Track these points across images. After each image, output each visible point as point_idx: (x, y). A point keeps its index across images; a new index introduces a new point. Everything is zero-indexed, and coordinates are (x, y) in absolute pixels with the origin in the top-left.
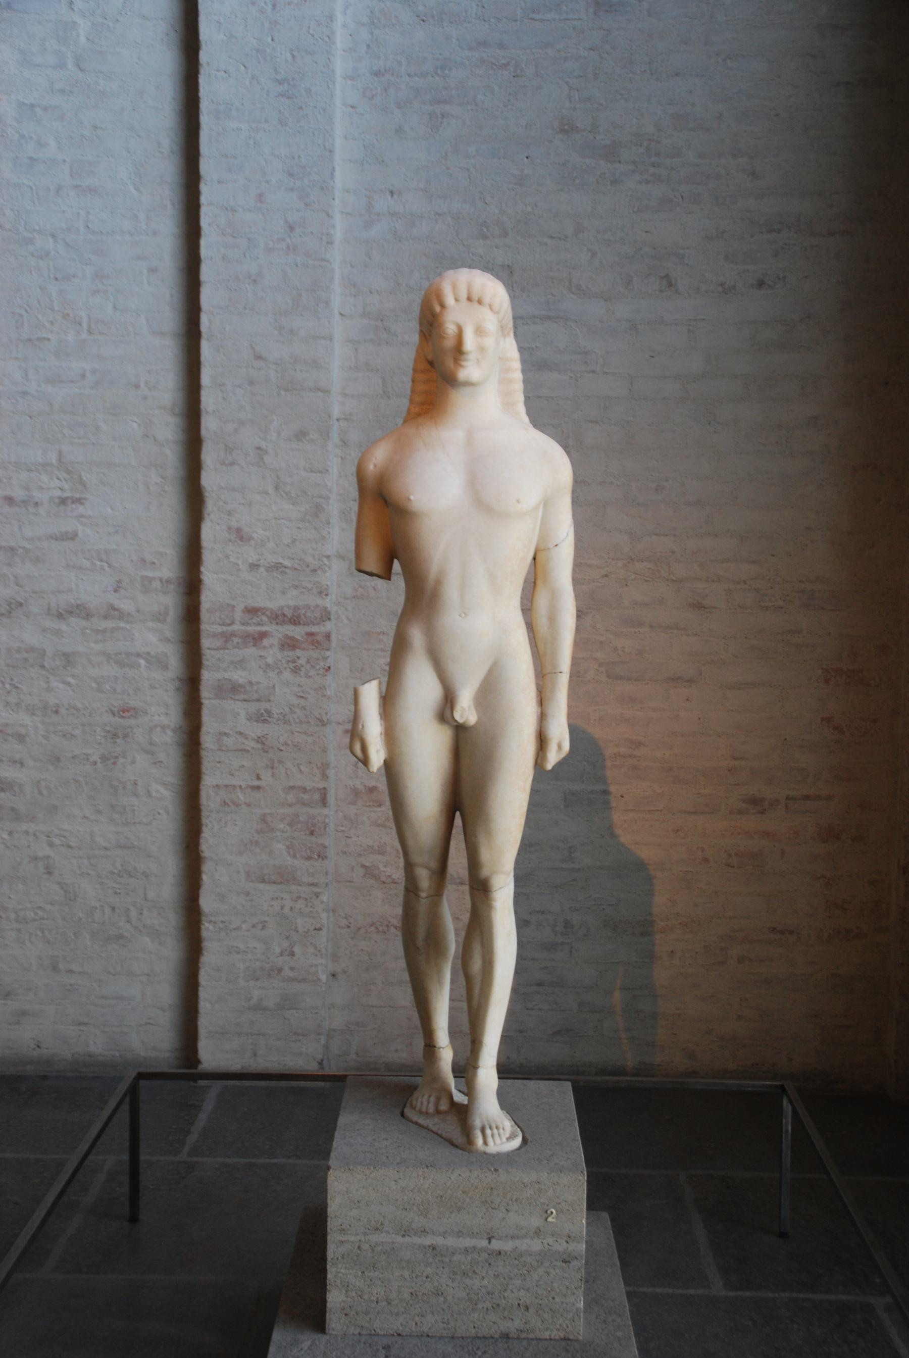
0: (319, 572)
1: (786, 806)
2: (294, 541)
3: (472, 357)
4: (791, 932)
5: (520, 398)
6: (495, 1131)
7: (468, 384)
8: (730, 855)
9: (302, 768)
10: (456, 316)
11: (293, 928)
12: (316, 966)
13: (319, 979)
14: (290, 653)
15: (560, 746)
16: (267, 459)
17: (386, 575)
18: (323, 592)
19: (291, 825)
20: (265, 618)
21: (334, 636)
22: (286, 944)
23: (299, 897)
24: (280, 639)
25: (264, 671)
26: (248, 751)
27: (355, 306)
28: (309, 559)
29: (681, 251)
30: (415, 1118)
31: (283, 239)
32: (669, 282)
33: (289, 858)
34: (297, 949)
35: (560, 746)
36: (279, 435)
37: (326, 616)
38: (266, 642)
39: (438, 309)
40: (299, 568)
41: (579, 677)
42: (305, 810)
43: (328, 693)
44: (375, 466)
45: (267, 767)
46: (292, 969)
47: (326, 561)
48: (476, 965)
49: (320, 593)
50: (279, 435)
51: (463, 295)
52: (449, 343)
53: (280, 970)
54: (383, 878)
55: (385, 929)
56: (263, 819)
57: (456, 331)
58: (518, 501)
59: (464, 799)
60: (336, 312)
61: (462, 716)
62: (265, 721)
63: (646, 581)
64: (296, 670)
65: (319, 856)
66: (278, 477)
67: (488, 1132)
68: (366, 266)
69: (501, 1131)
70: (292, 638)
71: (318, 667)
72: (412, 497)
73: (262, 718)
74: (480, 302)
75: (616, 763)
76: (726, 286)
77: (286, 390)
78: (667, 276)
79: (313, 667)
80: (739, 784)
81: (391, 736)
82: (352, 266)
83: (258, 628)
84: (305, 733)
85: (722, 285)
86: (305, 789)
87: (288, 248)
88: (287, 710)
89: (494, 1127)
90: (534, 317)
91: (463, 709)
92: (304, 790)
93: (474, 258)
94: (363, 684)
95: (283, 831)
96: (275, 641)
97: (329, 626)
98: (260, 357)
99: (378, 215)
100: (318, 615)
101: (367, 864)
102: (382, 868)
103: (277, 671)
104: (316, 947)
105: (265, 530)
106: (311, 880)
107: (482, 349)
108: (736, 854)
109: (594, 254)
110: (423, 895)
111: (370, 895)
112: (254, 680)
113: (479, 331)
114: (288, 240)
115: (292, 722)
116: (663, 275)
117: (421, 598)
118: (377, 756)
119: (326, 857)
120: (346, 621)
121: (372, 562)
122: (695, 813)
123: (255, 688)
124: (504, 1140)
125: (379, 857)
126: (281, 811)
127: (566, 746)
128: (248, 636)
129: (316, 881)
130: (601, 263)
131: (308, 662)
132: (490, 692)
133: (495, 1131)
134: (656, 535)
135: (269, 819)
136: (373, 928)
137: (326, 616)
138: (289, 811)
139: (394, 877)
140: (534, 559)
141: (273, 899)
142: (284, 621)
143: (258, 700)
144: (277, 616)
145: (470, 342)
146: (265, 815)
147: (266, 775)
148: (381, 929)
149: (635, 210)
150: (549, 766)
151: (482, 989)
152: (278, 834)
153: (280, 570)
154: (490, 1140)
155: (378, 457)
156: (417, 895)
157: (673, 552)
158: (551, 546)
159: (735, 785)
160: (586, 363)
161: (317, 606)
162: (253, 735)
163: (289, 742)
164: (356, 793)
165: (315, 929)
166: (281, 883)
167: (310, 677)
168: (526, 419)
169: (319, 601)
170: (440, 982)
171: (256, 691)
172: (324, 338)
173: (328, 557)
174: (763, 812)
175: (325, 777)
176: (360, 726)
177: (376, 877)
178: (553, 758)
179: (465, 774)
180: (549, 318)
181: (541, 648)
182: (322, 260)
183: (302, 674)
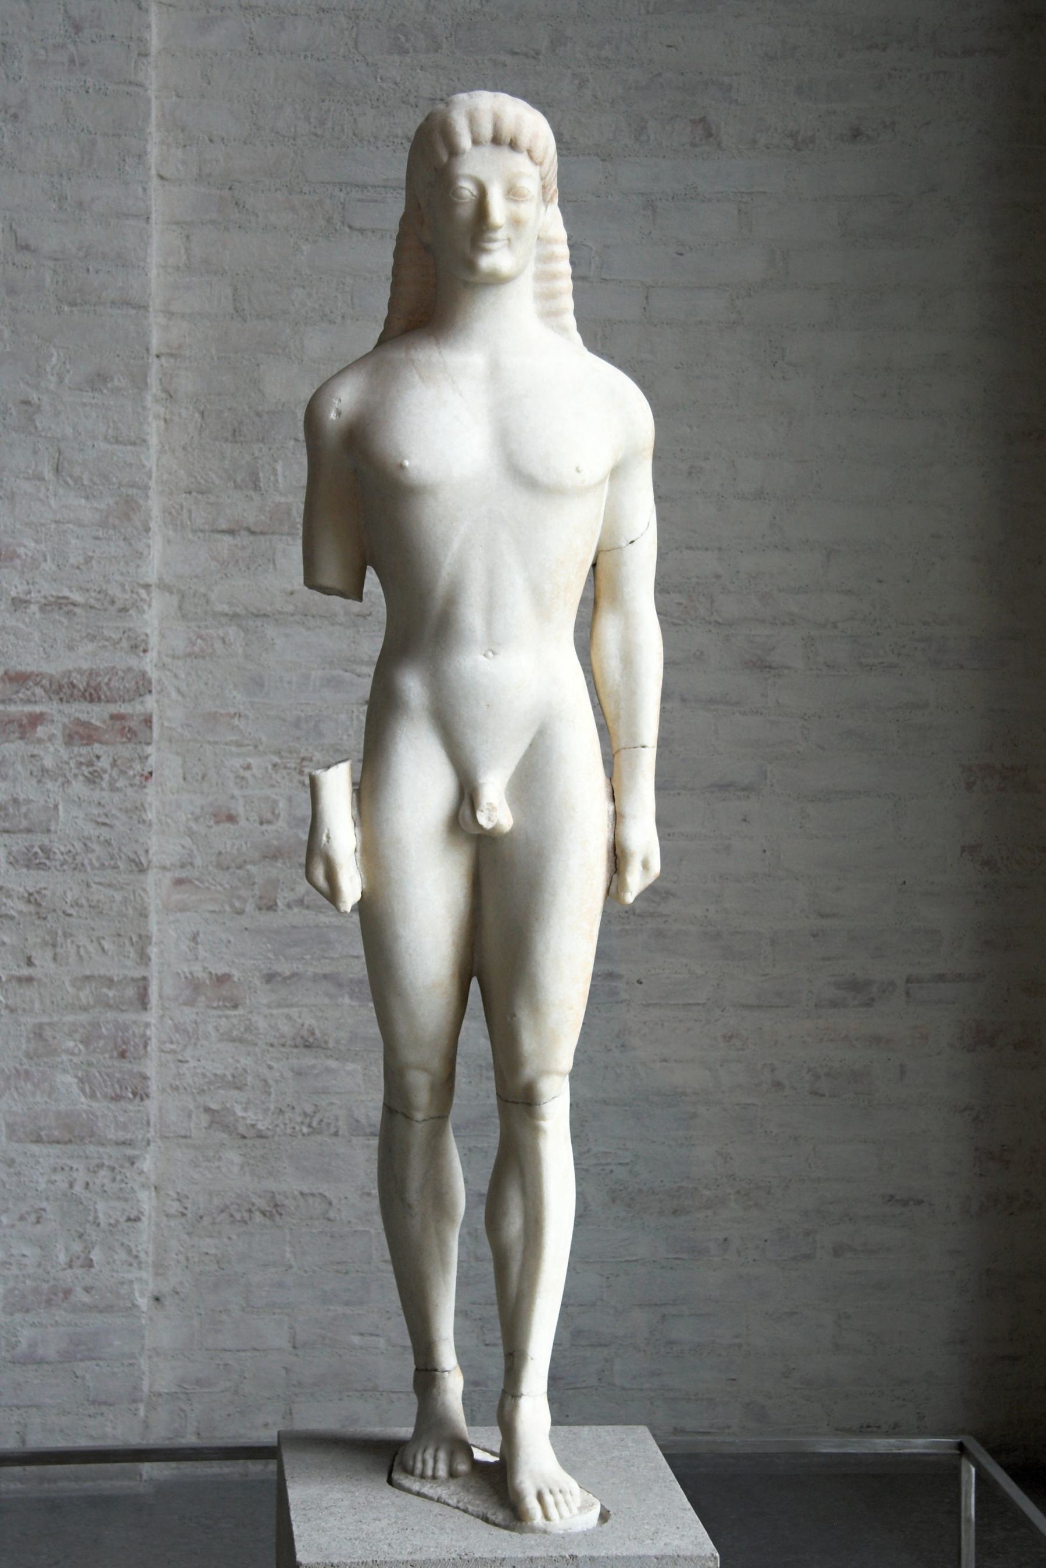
0: (132, 612)
1: (908, 993)
2: (88, 560)
3: (501, 235)
4: (920, 1202)
5: (568, 303)
6: (560, 1497)
7: (496, 280)
8: (817, 1077)
9: (106, 945)
10: (476, 166)
11: (91, 1218)
12: (131, 1282)
13: (135, 1306)
14: (84, 750)
15: (645, 865)
16: (40, 421)
18: (138, 646)
19: (86, 1042)
20: (38, 691)
21: (155, 719)
22: (77, 1247)
23: (101, 1166)
24: (65, 726)
25: (39, 782)
26: (12, 918)
27: (184, 163)
28: (113, 590)
29: (726, 80)
30: (416, 1486)
31: (63, 46)
32: (706, 130)
33: (83, 1099)
34: (96, 1255)
35: (645, 865)
36: (61, 380)
37: (143, 686)
38: (41, 731)
39: (445, 158)
40: (98, 606)
42: (110, 1015)
43: (150, 816)
44: (339, 413)
45: (45, 943)
46: (87, 1290)
47: (143, 593)
48: (514, 1225)
49: (134, 647)
50: (61, 380)
51: (486, 131)
52: (466, 211)
53: (68, 1293)
54: (242, 1130)
55: (246, 1215)
56: (38, 1033)
57: (475, 193)
58: (578, 471)
59: (495, 953)
60: (153, 172)
61: (489, 819)
62: (41, 866)
63: (674, 624)
64: (93, 779)
65: (135, 1094)
66: (60, 452)
67: (549, 1499)
68: (203, 96)
69: (569, 1496)
70: (87, 725)
71: (131, 773)
72: (407, 463)
73: (34, 860)
74: (513, 145)
75: (627, 927)
76: (800, 138)
77: (73, 304)
78: (703, 120)
79: (123, 772)
80: (829, 959)
82: (178, 96)
83: (28, 708)
84: (110, 885)
85: (793, 135)
86: (110, 981)
87: (72, 61)
88: (79, 846)
89: (556, 1490)
91: (492, 808)
92: (110, 982)
93: (385, 85)
94: (328, 767)
95: (73, 1054)
96: (56, 730)
97: (150, 703)
98: (27, 248)
99: (222, 9)
100: (131, 685)
101: (214, 1106)
102: (240, 1113)
103: (60, 780)
104: (129, 1251)
105: (37, 542)
106: (121, 1135)
107: (516, 223)
108: (827, 1075)
110: (419, 1116)
111: (220, 1159)
112: (22, 797)
113: (513, 193)
114: (72, 48)
115: (89, 868)
116: (697, 118)
117: (418, 627)
118: (351, 888)
119: (147, 1096)
120: (174, 695)
122: (760, 1007)
123: (24, 809)
124: (575, 1511)
125: (234, 1093)
126: (69, 1018)
127: (656, 867)
128: (11, 722)
129: (129, 1136)
130: (595, 97)
131: (114, 764)
132: (531, 780)
133: (560, 1497)
134: (691, 548)
135: (48, 1033)
136: (224, 1216)
137: (143, 686)
138: (83, 1018)
139: (260, 1126)
140: (594, 565)
141: (55, 1170)
142: (72, 695)
143: (29, 831)
144: (61, 687)
145: (498, 209)
146: (41, 1026)
147: (43, 959)
148: (238, 1216)
149: (650, 9)
150: (630, 898)
151: (523, 1265)
152: (65, 1057)
153: (65, 609)
154: (553, 1512)
155: (345, 399)
156: (408, 1117)
157: (718, 577)
158: (624, 544)
159: (824, 959)
161: (130, 669)
162: (21, 890)
163: (84, 901)
164: (195, 986)
165: (129, 1219)
166: (70, 1141)
167: (118, 790)
168: (578, 338)
169: (133, 662)
170: (444, 1264)
171: (26, 816)
172: (136, 216)
173: (147, 587)
174: (869, 1003)
175: (144, 958)
176: (324, 838)
177: (226, 1128)
178: (636, 883)
179: (490, 914)
181: (609, 708)
182: (131, 83)
183: (105, 784)
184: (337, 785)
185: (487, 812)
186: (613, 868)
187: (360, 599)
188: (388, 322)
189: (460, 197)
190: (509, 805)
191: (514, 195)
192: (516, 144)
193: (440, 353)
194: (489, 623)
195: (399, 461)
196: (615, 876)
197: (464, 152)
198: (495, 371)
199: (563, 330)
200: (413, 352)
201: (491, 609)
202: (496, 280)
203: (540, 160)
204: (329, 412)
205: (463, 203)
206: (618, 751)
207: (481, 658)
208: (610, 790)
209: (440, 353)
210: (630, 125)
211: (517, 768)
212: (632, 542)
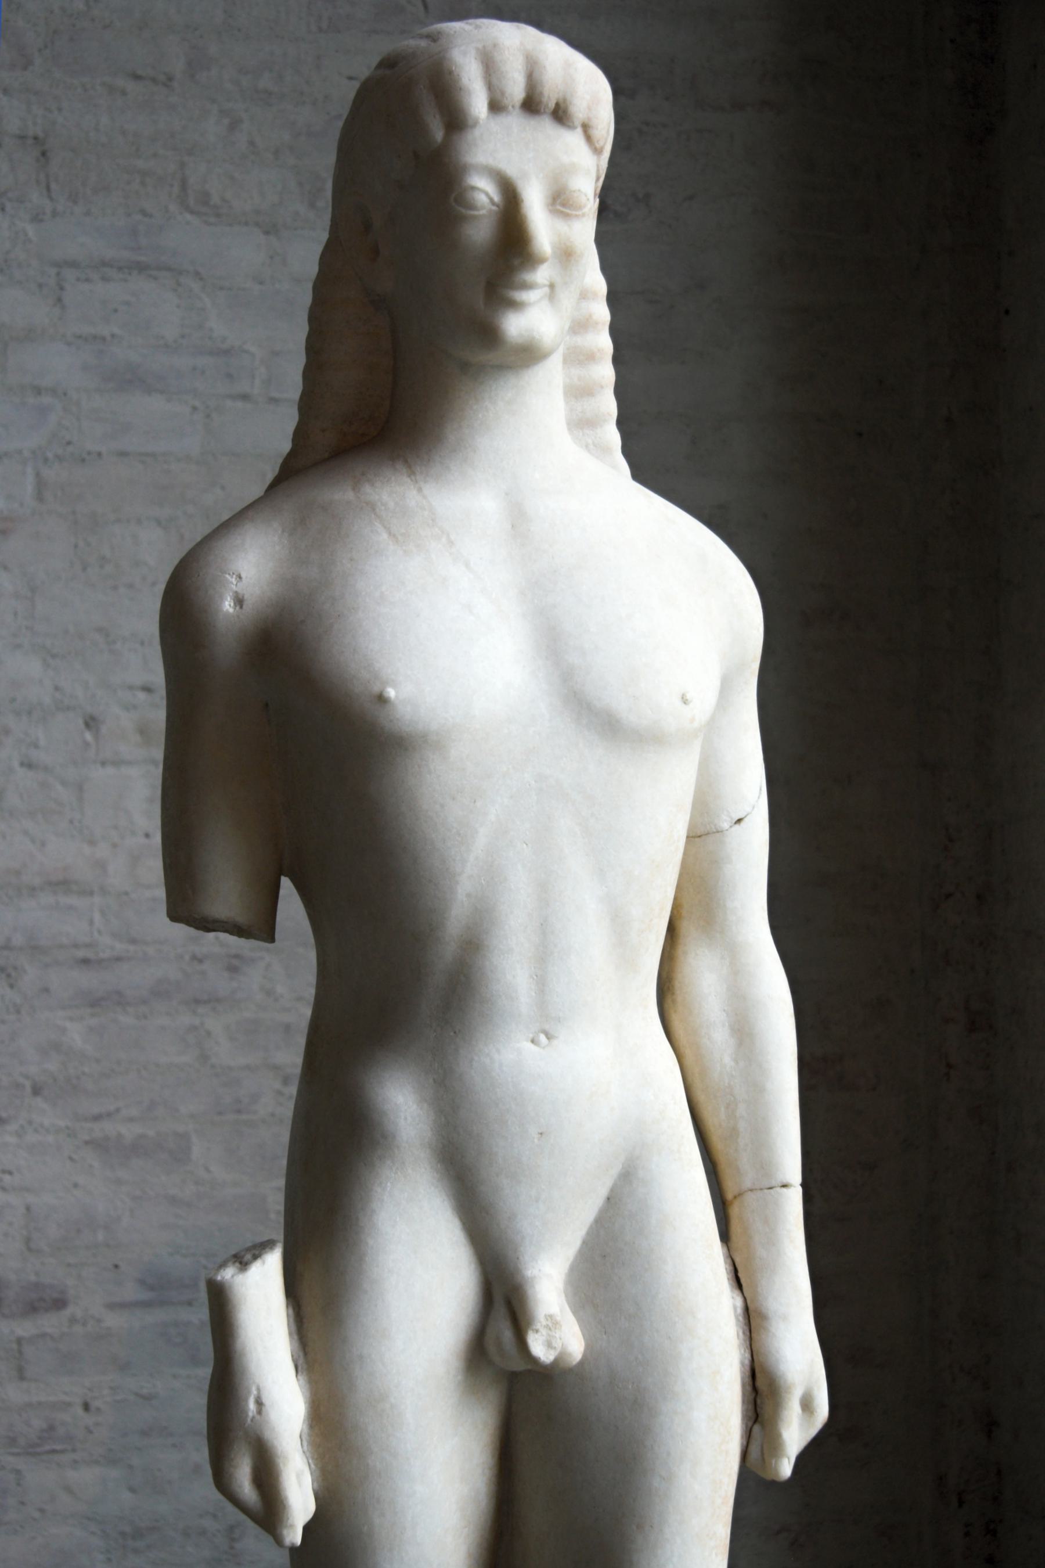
3: (542, 275)
7: (529, 354)
15: (807, 1405)
17: (263, 928)
35: (807, 1405)
41: (239, 1112)
44: (239, 601)
51: (516, 90)
52: (480, 232)
57: (497, 198)
58: (685, 701)
61: (549, 1345)
72: (391, 693)
74: (560, 115)
81: (334, 1425)
90: (104, 264)
91: (554, 1323)
107: (567, 255)
109: (234, 125)
113: (560, 202)
118: (300, 1501)
121: (226, 892)
130: (252, 143)
150: (786, 1469)
155: (248, 574)
158: (725, 825)
160: (229, 376)
180: (141, 268)
184: (261, 1293)
185: (544, 1331)
186: (751, 1413)
187: (270, 937)
188: (300, 435)
189: (472, 207)
190: (575, 1313)
191: (564, 205)
192: (565, 112)
193: (420, 490)
194: (542, 984)
195: (376, 689)
196: (757, 1428)
197: (476, 123)
198: (518, 521)
199: (600, 450)
200: (367, 489)
201: (544, 956)
202: (529, 354)
203: (601, 143)
204: (222, 598)
205: (475, 217)
206: (739, 1195)
207: (528, 1046)
208: (732, 1268)
209: (420, 490)
211: (585, 1243)
212: (739, 821)
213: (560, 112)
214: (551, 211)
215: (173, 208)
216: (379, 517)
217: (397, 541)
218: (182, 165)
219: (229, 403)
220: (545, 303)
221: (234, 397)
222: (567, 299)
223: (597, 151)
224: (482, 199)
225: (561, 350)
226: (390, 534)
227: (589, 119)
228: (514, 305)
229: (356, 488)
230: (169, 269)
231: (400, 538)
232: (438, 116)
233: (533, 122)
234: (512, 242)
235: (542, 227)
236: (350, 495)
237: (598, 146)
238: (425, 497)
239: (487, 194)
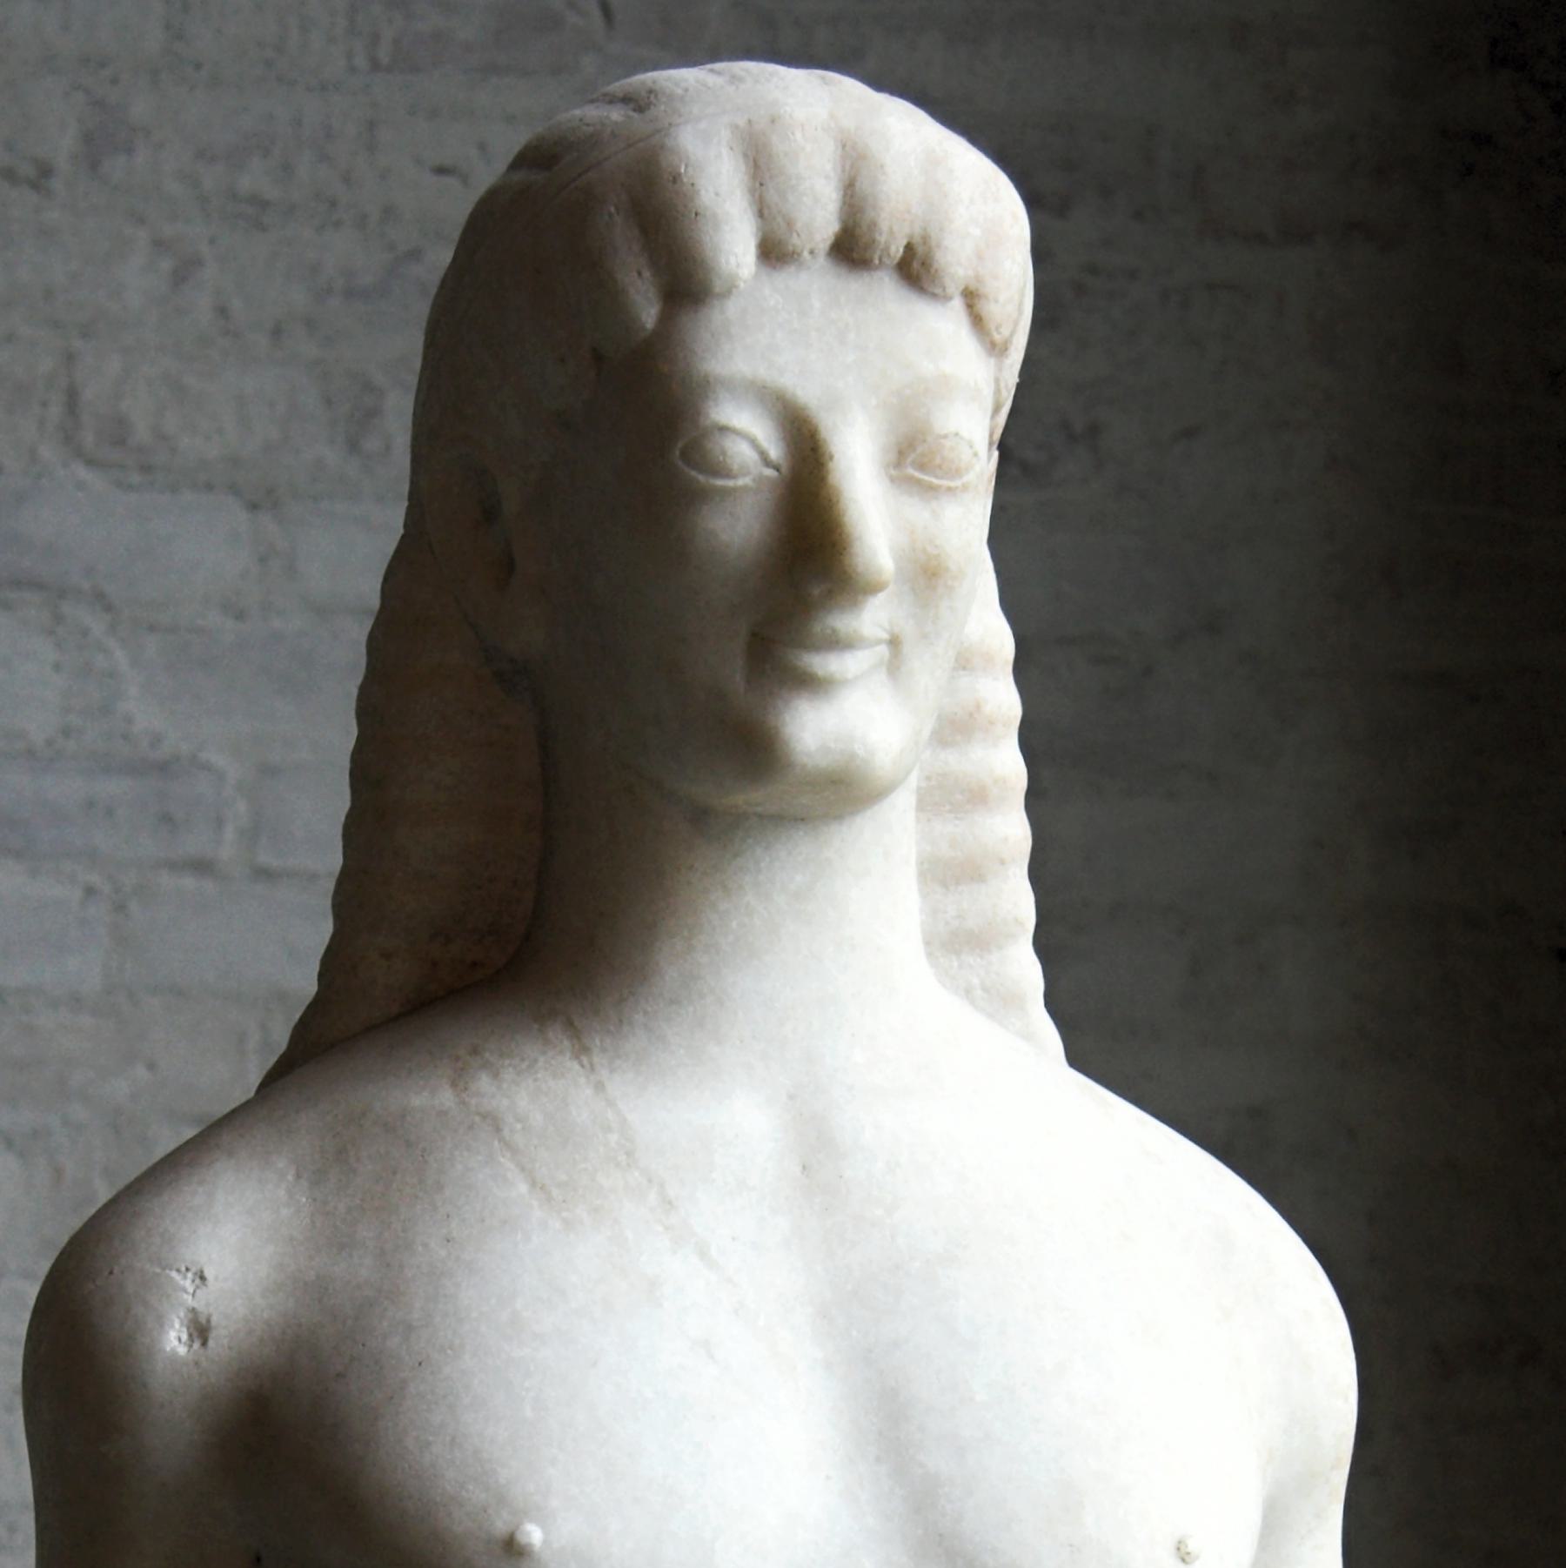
3: (871, 619)
7: (843, 792)
39: (648, 313)
51: (819, 218)
52: (737, 524)
57: (775, 452)
74: (915, 270)
107: (928, 575)
113: (914, 459)
130: (222, 311)
160: (167, 819)
188: (335, 964)
191: (922, 467)
192: (926, 264)
193: (599, 1087)
200: (484, 1082)
202: (843, 792)
203: (1005, 332)
205: (726, 493)
209: (599, 1087)
210: (329, 402)
213: (916, 265)
214: (892, 480)
215: (47, 452)
216: (508, 1146)
217: (549, 1199)
218: (70, 358)
219: (166, 880)
220: (882, 676)
221: (174, 866)
222: (927, 670)
223: (996, 349)
224: (740, 454)
225: (913, 780)
226: (533, 1184)
227: (978, 279)
228: (809, 683)
229: (459, 1080)
230: (38, 585)
231: (555, 1192)
232: (647, 274)
233: (855, 285)
234: (808, 547)
235: (874, 514)
236: (446, 1097)
237: (997, 337)
238: (611, 1103)
239: (754, 443)
